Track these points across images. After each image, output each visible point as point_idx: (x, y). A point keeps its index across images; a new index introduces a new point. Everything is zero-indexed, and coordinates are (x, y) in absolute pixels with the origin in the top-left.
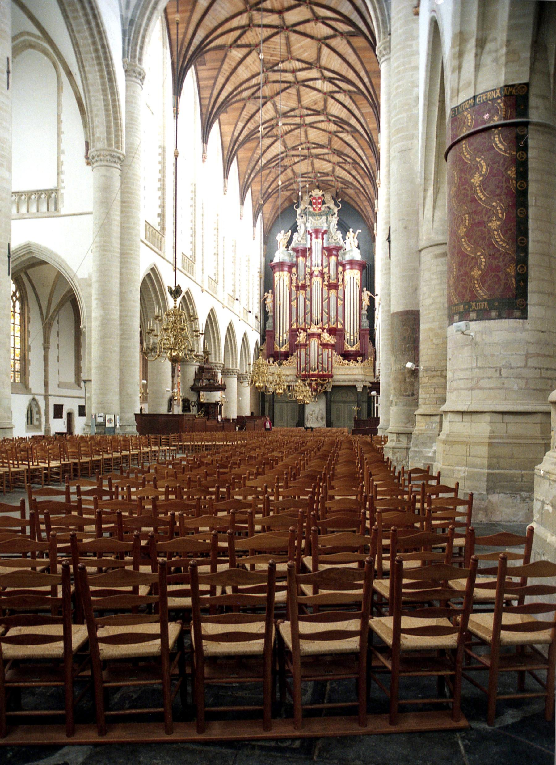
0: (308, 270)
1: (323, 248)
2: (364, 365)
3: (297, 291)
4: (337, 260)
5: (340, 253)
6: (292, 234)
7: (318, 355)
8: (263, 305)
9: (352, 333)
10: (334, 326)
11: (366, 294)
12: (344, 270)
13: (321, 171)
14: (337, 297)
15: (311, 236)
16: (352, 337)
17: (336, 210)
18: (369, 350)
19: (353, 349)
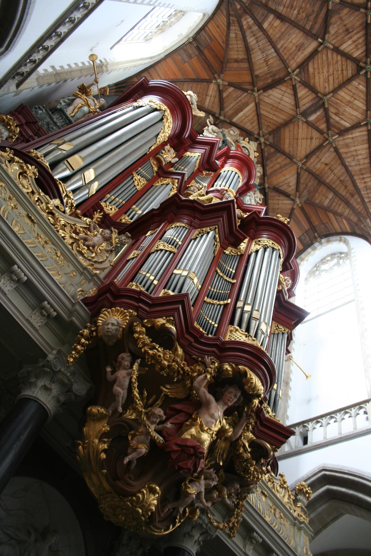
13: (332, 110)
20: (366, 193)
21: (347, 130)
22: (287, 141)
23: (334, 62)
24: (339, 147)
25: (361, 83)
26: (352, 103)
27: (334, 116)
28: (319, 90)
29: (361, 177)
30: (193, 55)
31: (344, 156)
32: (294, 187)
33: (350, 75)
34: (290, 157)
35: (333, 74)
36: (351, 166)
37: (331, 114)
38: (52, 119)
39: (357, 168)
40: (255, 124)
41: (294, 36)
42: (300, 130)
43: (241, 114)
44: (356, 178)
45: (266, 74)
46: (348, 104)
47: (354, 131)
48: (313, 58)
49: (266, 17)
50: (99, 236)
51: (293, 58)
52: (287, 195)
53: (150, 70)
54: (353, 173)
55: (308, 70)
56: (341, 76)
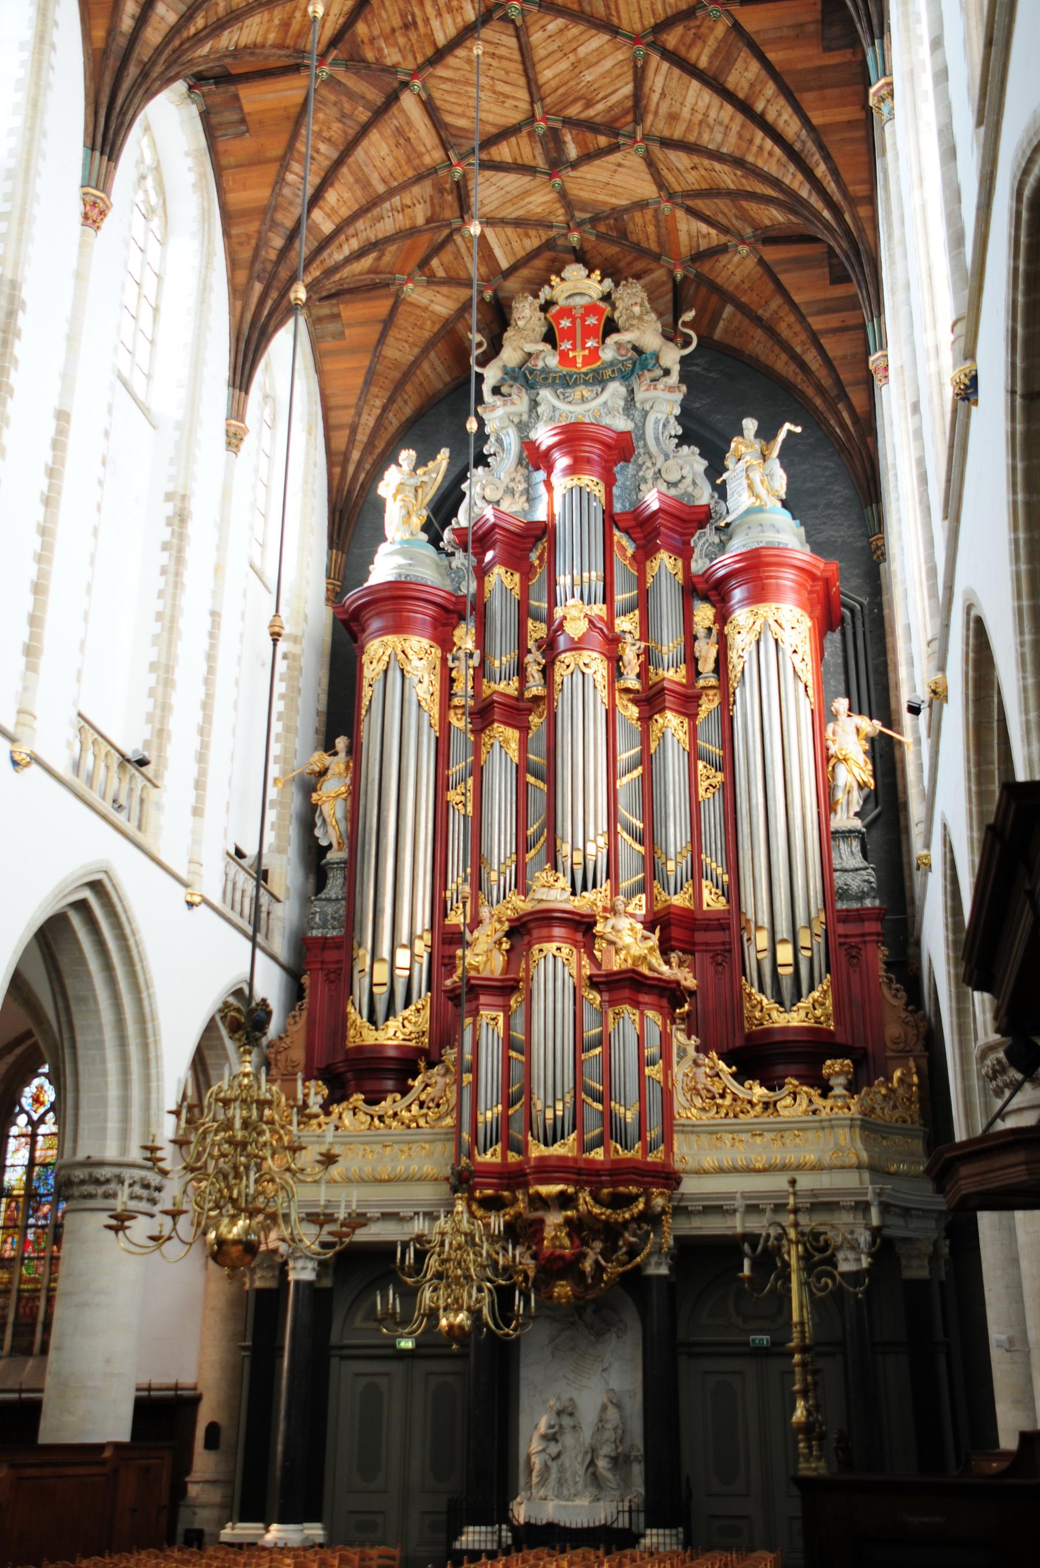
0: (537, 630)
1: (610, 519)
2: (867, 1112)
3: (478, 732)
4: (687, 568)
5: (703, 540)
6: (457, 478)
7: (580, 1046)
8: (309, 818)
9: (783, 930)
10: (680, 900)
11: (851, 734)
12: (723, 617)
13: (573, 111)
14: (694, 755)
15: (550, 470)
16: (785, 954)
17: (672, 356)
18: (893, 1030)
19: (795, 1019)
20: (790, 177)
21: (638, 97)
22: (602, 198)
23: (468, 67)
24: (666, 133)
25: (543, 22)
26: (579, 61)
27: (591, 112)
28: (514, 122)
29: (754, 149)
30: (335, 310)
31: (692, 138)
32: (713, 232)
33: (513, 42)
34: (641, 205)
35: (492, 78)
36: (722, 144)
37: (583, 116)
38: (328, 900)
39: (733, 138)
40: (533, 233)
41: (373, 151)
42: (589, 176)
43: (498, 252)
44: (750, 158)
45: (433, 205)
46: (577, 70)
47: (648, 84)
48: (438, 109)
49: (314, 228)
50: (439, 1079)
51: (420, 156)
52: (723, 249)
53: (332, 421)
54: (737, 154)
55: (461, 129)
56: (505, 64)
